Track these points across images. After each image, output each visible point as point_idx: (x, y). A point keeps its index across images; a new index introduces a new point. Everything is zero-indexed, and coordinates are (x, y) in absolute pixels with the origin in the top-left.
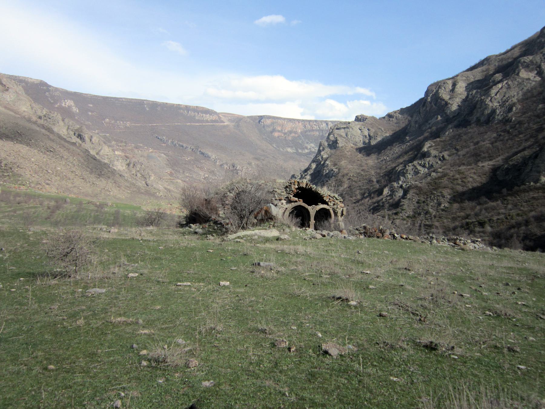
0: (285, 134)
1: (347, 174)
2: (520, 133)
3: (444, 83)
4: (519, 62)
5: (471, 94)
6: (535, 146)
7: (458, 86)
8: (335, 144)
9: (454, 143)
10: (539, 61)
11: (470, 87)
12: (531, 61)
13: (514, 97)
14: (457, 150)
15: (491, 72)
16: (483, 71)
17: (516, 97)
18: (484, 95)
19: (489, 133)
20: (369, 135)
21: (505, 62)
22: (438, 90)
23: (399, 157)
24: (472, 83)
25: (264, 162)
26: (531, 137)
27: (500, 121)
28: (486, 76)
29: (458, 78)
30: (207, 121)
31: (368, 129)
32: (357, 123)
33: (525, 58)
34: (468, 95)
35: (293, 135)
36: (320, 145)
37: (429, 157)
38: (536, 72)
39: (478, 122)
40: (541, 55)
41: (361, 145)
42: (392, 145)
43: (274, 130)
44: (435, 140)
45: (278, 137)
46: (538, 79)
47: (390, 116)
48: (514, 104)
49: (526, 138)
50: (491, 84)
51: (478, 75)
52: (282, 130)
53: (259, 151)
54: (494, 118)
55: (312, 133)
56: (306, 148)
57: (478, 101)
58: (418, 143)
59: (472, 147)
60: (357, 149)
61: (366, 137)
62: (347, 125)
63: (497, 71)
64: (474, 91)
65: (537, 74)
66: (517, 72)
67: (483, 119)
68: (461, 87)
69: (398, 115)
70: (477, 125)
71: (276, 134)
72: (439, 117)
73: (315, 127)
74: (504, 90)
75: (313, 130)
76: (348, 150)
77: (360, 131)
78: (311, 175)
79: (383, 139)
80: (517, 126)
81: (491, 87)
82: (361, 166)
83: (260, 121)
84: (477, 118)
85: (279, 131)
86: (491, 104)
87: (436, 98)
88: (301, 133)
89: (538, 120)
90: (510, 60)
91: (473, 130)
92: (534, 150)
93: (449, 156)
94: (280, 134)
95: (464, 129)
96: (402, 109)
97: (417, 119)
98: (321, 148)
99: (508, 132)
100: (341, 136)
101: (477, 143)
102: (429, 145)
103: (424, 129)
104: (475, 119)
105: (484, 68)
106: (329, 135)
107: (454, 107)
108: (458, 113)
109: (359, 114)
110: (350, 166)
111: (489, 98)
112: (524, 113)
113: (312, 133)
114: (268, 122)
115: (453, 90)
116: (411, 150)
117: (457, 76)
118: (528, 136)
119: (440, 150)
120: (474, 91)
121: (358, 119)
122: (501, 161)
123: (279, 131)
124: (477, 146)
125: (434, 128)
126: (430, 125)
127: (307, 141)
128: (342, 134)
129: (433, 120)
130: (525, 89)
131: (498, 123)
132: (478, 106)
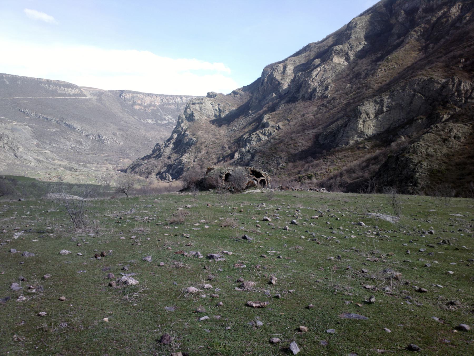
0: (145, 107)
3: (277, 67)
4: (333, 49)
5: (298, 76)
6: (345, 118)
7: (287, 69)
8: (191, 117)
9: (286, 116)
10: (347, 50)
11: (296, 70)
12: (341, 50)
14: (289, 121)
15: (312, 58)
16: (306, 57)
17: (331, 78)
18: (307, 77)
19: (311, 107)
20: (219, 109)
21: (322, 50)
22: (272, 72)
23: (244, 128)
25: (128, 132)
27: (319, 98)
29: (288, 62)
30: (69, 95)
31: (218, 104)
32: (209, 99)
34: (295, 76)
35: (152, 108)
36: (179, 118)
37: (268, 127)
38: (344, 58)
39: (304, 99)
40: (348, 45)
43: (134, 104)
44: (272, 113)
45: (139, 110)
46: (346, 63)
47: (235, 93)
48: (329, 84)
49: (338, 110)
50: (312, 67)
51: (301, 60)
52: (142, 104)
54: (315, 95)
55: (169, 106)
56: (165, 119)
57: (303, 81)
58: (258, 115)
59: (300, 119)
60: (210, 121)
62: (200, 100)
64: (300, 73)
65: (345, 60)
66: (331, 58)
68: (290, 69)
69: (241, 92)
70: (303, 100)
71: (137, 107)
72: (274, 94)
73: (172, 101)
74: (322, 72)
75: (170, 104)
76: (203, 122)
79: (230, 112)
80: (332, 101)
81: (312, 70)
82: (215, 135)
83: (120, 95)
84: (303, 95)
85: (139, 105)
86: (312, 84)
87: (272, 79)
88: (159, 106)
89: (347, 97)
90: (326, 48)
91: (300, 105)
92: (345, 120)
93: (283, 125)
94: (140, 107)
95: (293, 104)
96: (244, 87)
97: (257, 95)
98: (180, 121)
99: (326, 106)
100: (196, 110)
101: (303, 115)
102: (267, 117)
103: (263, 104)
104: (301, 95)
105: (307, 54)
106: (186, 109)
107: (285, 86)
108: (288, 92)
110: (206, 136)
111: (311, 79)
112: (337, 91)
113: (169, 106)
114: (129, 96)
115: (284, 72)
116: (254, 121)
117: (286, 60)
118: (340, 109)
119: (276, 121)
120: (300, 73)
121: (209, 95)
123: (139, 105)
124: (303, 118)
125: (271, 103)
126: (268, 101)
127: (165, 113)
128: (197, 108)
129: (270, 96)
130: (337, 71)
131: (318, 99)
132: (303, 85)
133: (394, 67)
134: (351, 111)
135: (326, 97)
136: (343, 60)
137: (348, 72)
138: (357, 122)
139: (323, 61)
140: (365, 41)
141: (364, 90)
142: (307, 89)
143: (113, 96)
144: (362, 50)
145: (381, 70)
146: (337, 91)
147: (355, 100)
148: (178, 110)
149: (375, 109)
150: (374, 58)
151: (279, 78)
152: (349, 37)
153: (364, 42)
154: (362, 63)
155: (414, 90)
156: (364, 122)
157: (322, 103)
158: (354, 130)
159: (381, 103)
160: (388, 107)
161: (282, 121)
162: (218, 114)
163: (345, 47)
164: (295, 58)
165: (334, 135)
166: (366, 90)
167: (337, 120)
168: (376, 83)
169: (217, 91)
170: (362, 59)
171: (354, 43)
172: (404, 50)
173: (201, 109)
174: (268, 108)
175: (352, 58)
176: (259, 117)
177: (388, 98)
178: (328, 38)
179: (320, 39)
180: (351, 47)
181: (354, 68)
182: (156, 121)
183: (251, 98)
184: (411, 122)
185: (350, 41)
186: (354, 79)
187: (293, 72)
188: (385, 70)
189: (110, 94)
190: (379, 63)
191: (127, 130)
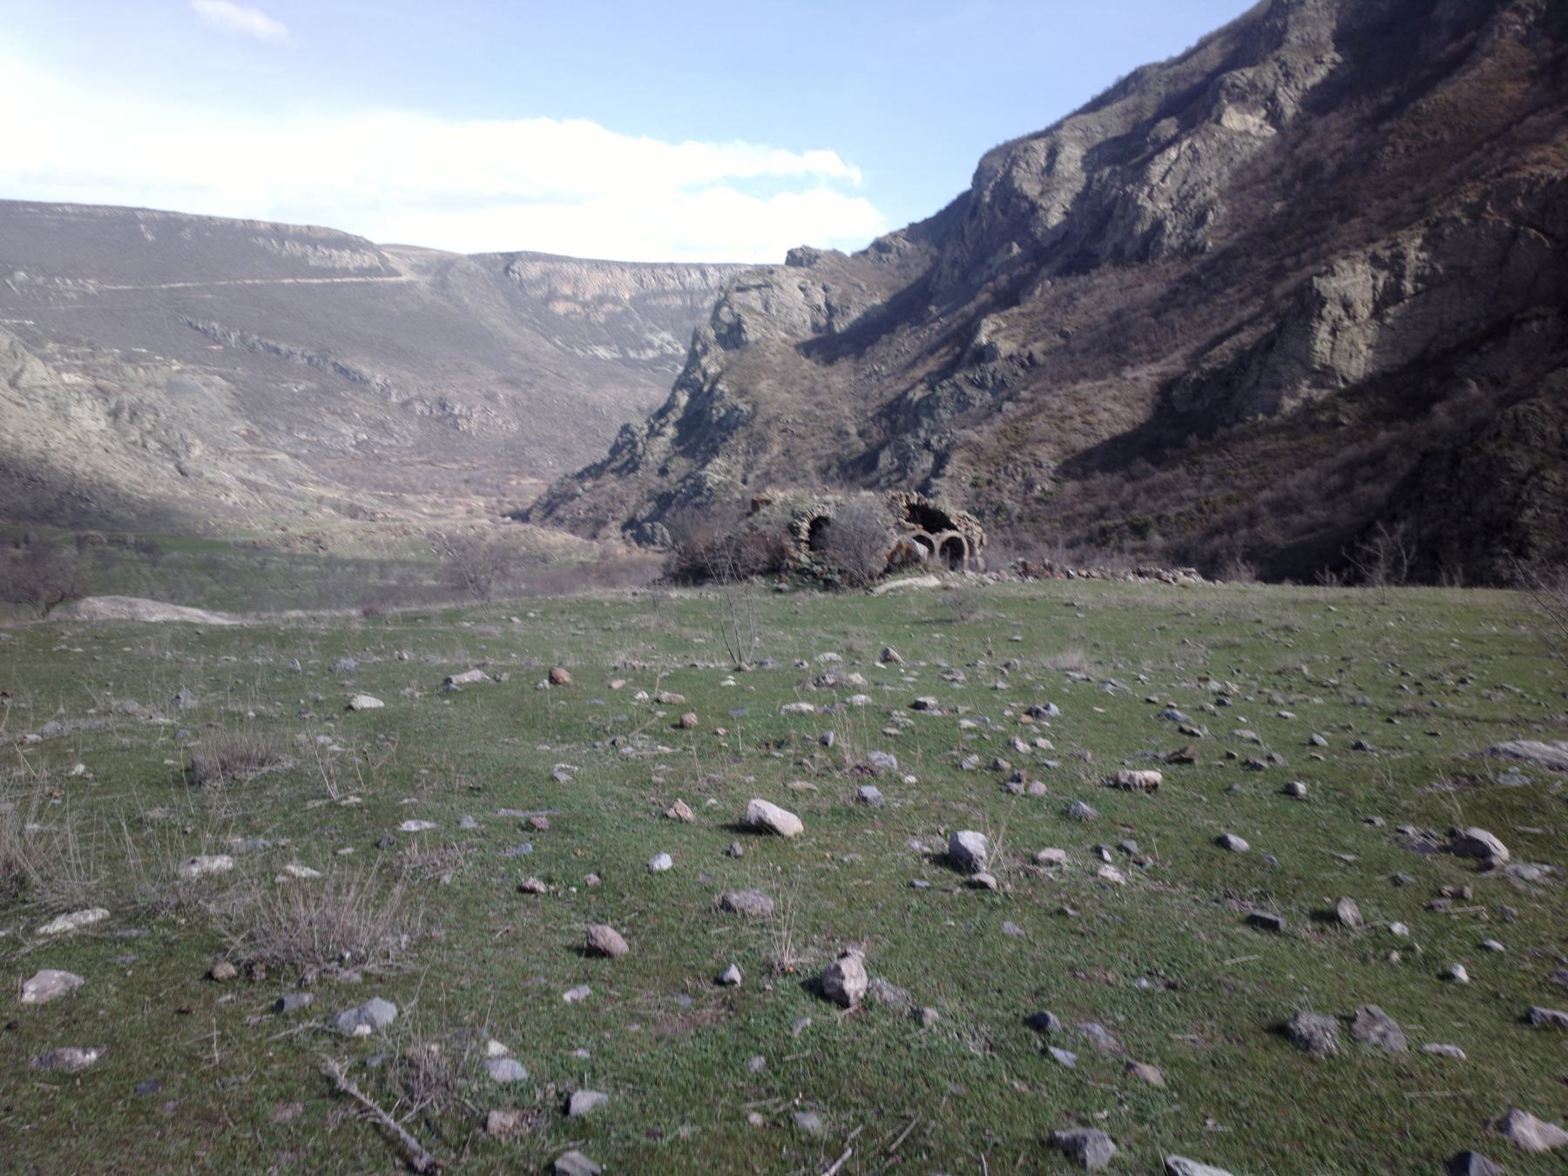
0: (585, 305)
1: (777, 418)
2: (1228, 283)
3: (1026, 150)
5: (1099, 180)
6: (1265, 319)
7: (1062, 157)
8: (735, 334)
9: (1057, 319)
10: (1270, 83)
11: (1093, 160)
13: (1209, 184)
15: (1149, 115)
16: (1127, 112)
17: (1215, 184)
18: (1133, 182)
20: (828, 305)
21: (1183, 86)
24: (1099, 147)
26: (1257, 292)
27: (1175, 253)
28: (1136, 126)
29: (1063, 133)
30: (346, 272)
31: (825, 289)
32: (792, 270)
33: (1236, 73)
34: (1090, 180)
35: (609, 307)
36: (696, 337)
38: (1263, 113)
39: (1119, 258)
41: (807, 334)
42: (893, 332)
43: (552, 296)
44: (1006, 313)
45: (566, 316)
46: (1270, 131)
47: (880, 246)
48: (1210, 204)
50: (1150, 149)
51: (1113, 123)
53: (513, 358)
54: (1159, 243)
55: (664, 301)
56: (651, 345)
57: (1116, 198)
58: (961, 321)
60: (797, 347)
61: (819, 310)
62: (764, 276)
63: (1164, 112)
64: (1107, 171)
65: (1266, 119)
66: (1215, 113)
67: (1129, 247)
68: (1072, 157)
70: (1116, 264)
71: (560, 308)
73: (671, 284)
74: (1185, 165)
75: (665, 293)
76: (773, 350)
77: (801, 295)
78: (678, 424)
79: (866, 314)
80: (1220, 263)
81: (1151, 158)
82: (812, 392)
83: (507, 269)
84: (1115, 246)
85: (567, 298)
86: (1149, 206)
87: (1007, 193)
88: (633, 301)
90: (1197, 80)
92: (1264, 329)
93: (1045, 353)
94: (571, 306)
95: (1082, 278)
96: (913, 226)
98: (699, 347)
100: (751, 310)
102: (992, 327)
104: (1109, 248)
105: (1130, 101)
106: (718, 306)
107: (1055, 218)
108: (1063, 235)
109: (796, 244)
110: (783, 396)
111: (1146, 190)
113: (664, 301)
114: (534, 271)
115: (1049, 169)
116: (945, 341)
117: (1058, 126)
118: (1249, 290)
119: (1021, 339)
120: (1107, 171)
121: (794, 259)
122: (1181, 362)
123: (567, 298)
125: (1003, 279)
130: (1238, 159)
131: (1170, 258)
132: (1117, 212)
133: (1442, 140)
134: (1286, 296)
135: (1197, 250)
136: (1257, 121)
137: (1275, 161)
138: (1308, 334)
139: (1189, 125)
140: (1336, 50)
141: (1335, 221)
142: (1133, 223)
143: (484, 271)
144: (1325, 83)
145: (1395, 152)
146: (1236, 227)
147: (1304, 256)
148: (693, 312)
149: (1374, 288)
150: (1367, 108)
151: (1031, 188)
152: (1277, 39)
153: (1331, 56)
154: (1326, 129)
155: (1516, 218)
156: (1333, 332)
157: (1186, 269)
158: (1300, 361)
159: (1396, 265)
160: (1418, 278)
161: (1044, 337)
162: (823, 321)
163: (1267, 74)
164: (1090, 118)
165: (1226, 381)
166: (1342, 221)
167: (1238, 329)
168: (1377, 197)
169: (820, 243)
170: (1325, 113)
171: (1298, 61)
172: (1478, 79)
173: (766, 306)
174: (995, 294)
175: (1290, 111)
176: (960, 328)
177: (1421, 249)
178: (1204, 44)
179: (1177, 51)
180: (1287, 75)
181: (1295, 146)
182: (623, 351)
183: (936, 262)
184: (1501, 329)
185: (1284, 53)
186: (1298, 186)
187: (1083, 169)
188: (1407, 148)
189: (473, 266)
190: (1387, 125)
191: (530, 385)
